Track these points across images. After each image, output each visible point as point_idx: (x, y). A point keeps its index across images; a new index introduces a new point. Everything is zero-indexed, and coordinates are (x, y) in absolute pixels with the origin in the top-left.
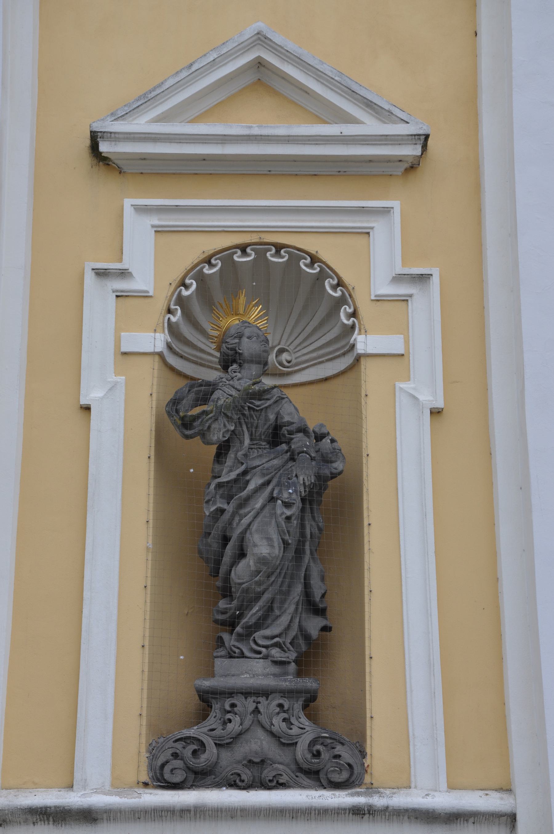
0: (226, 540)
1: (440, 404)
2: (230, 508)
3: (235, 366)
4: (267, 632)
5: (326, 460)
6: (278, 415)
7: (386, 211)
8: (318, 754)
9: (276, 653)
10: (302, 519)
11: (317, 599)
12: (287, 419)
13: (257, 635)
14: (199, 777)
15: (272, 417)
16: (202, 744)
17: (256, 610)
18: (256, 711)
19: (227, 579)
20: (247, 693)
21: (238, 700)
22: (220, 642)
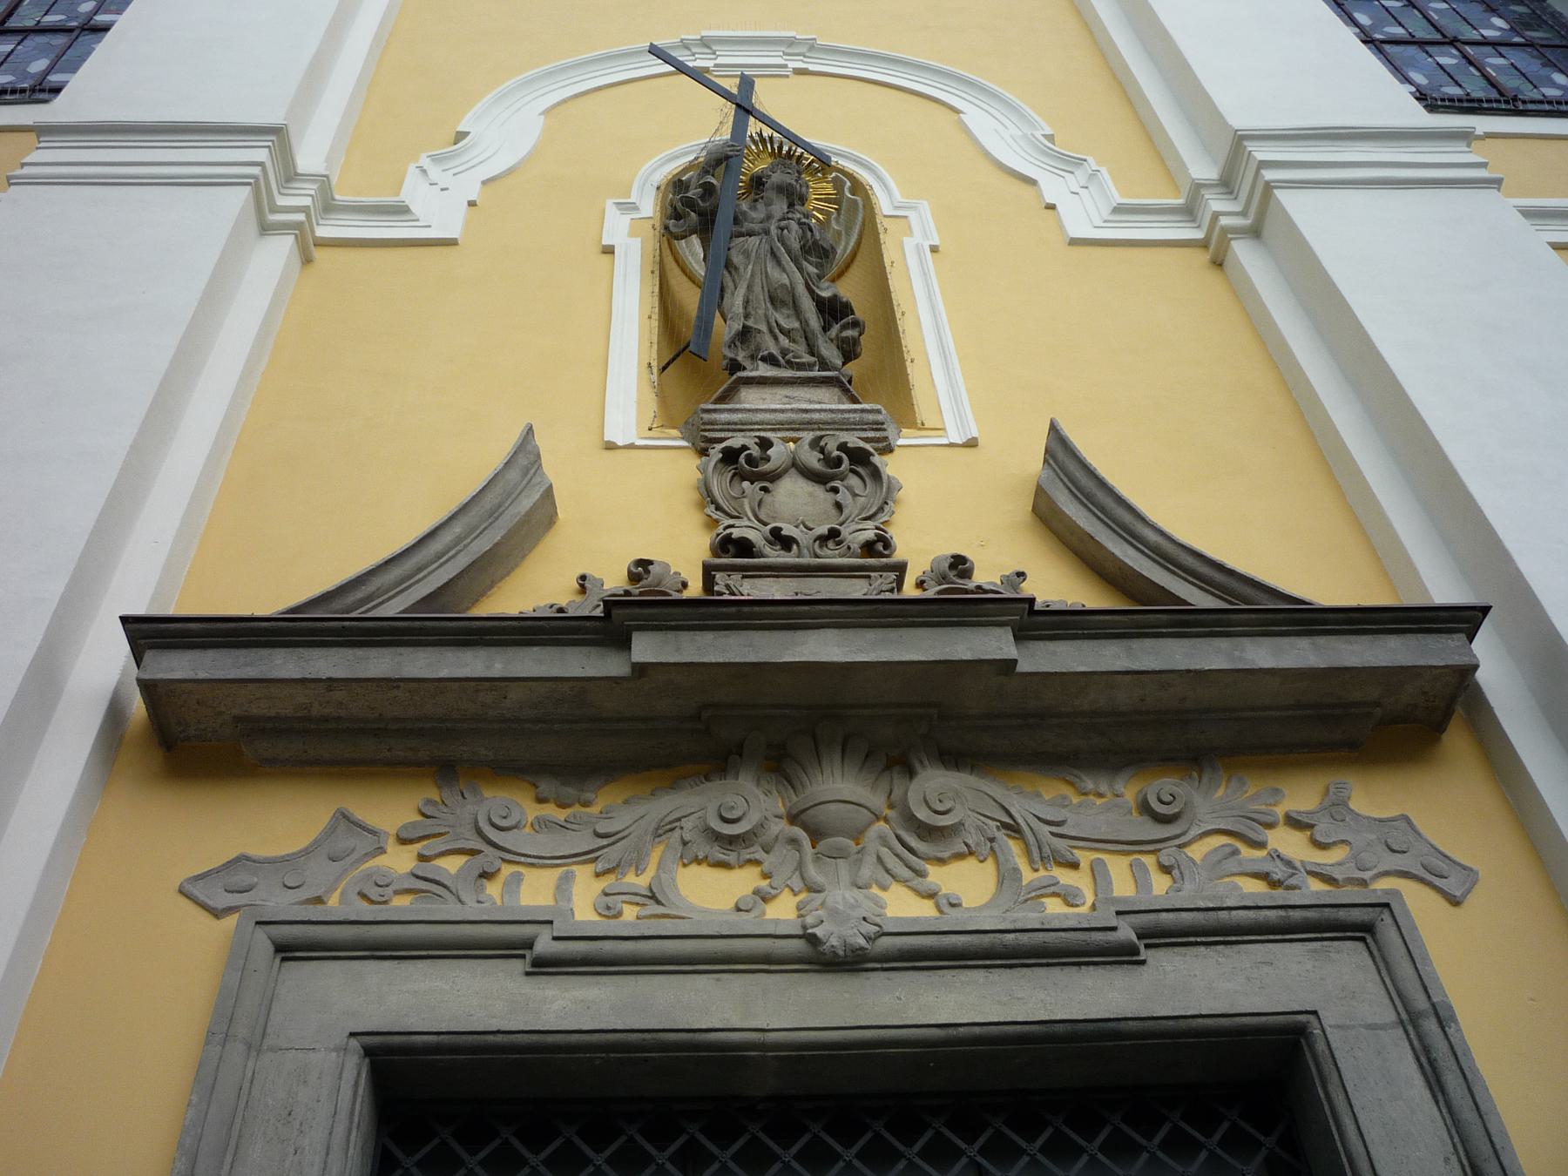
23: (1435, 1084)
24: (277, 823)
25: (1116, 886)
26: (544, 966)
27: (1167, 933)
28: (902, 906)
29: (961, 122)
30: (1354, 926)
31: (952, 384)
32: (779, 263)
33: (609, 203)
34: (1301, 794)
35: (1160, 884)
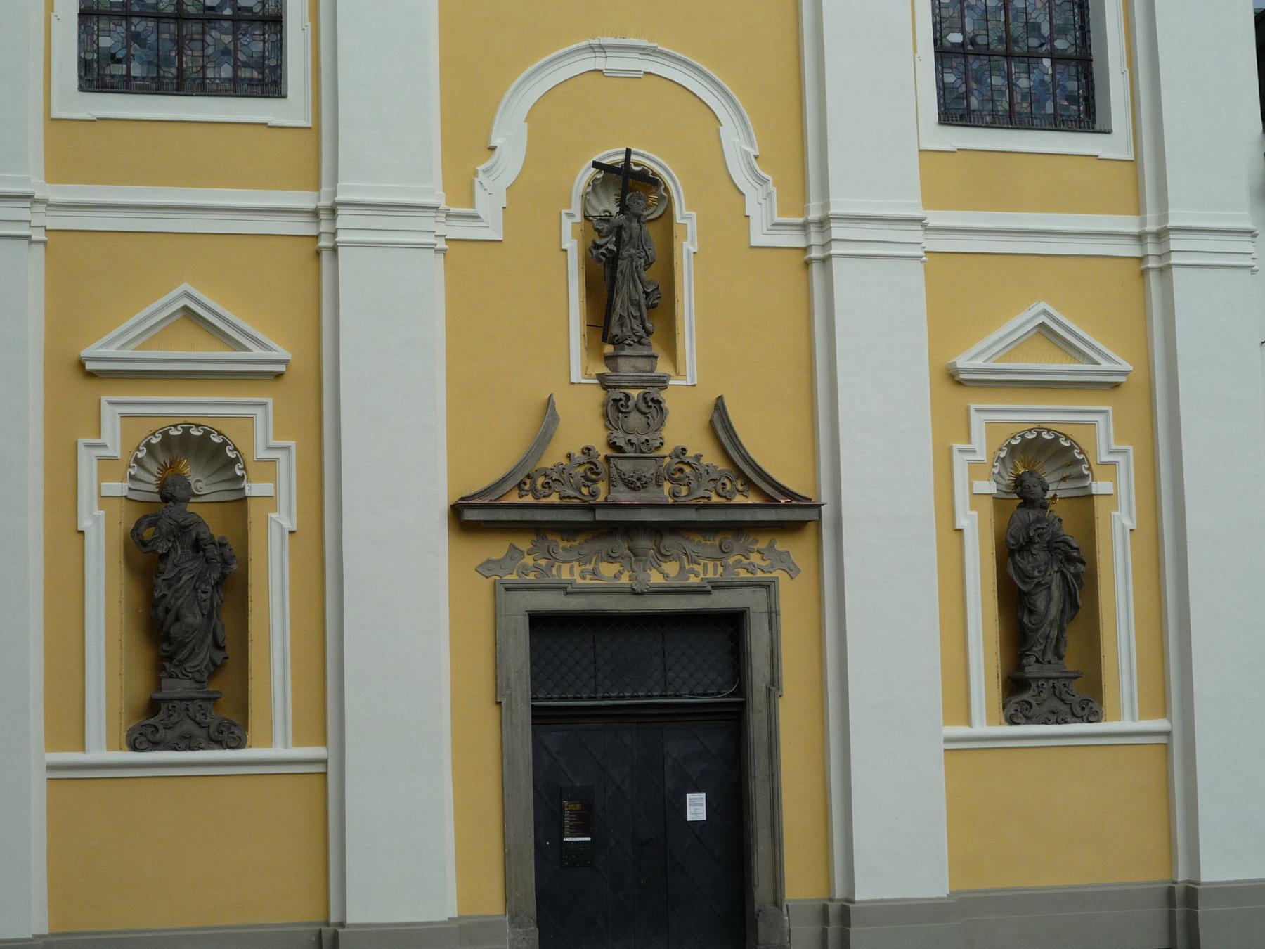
0: (167, 611)
1: (294, 528)
2: (170, 594)
3: (171, 503)
4: (192, 664)
5: (226, 562)
6: (198, 534)
7: (264, 405)
8: (222, 732)
9: (197, 675)
10: (212, 598)
11: (220, 641)
12: (202, 536)
13: (186, 665)
14: (156, 745)
15: (194, 535)
16: (156, 728)
17: (186, 651)
18: (187, 709)
19: (168, 633)
20: (181, 700)
21: (177, 703)
22: (164, 668)
23: (770, 629)
24: (495, 548)
25: (709, 571)
26: (568, 594)
27: (716, 587)
28: (656, 578)
29: (718, 131)
30: (767, 586)
31: (691, 349)
32: (635, 286)
33: (563, 211)
34: (762, 543)
35: (720, 570)
